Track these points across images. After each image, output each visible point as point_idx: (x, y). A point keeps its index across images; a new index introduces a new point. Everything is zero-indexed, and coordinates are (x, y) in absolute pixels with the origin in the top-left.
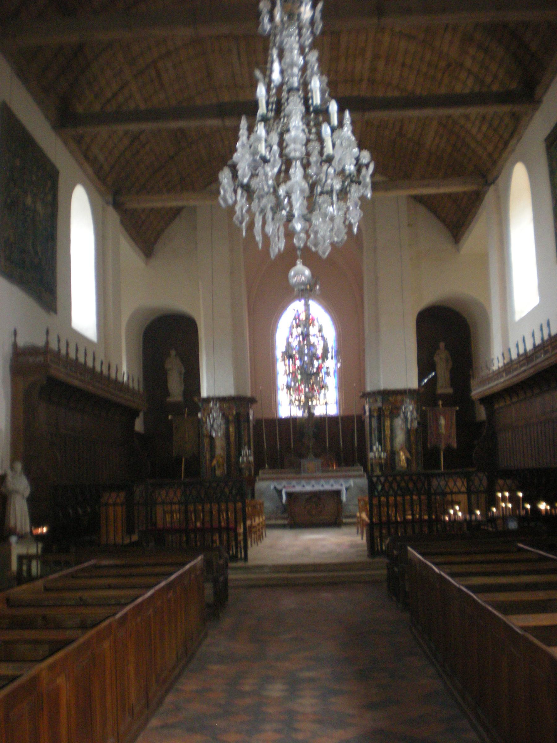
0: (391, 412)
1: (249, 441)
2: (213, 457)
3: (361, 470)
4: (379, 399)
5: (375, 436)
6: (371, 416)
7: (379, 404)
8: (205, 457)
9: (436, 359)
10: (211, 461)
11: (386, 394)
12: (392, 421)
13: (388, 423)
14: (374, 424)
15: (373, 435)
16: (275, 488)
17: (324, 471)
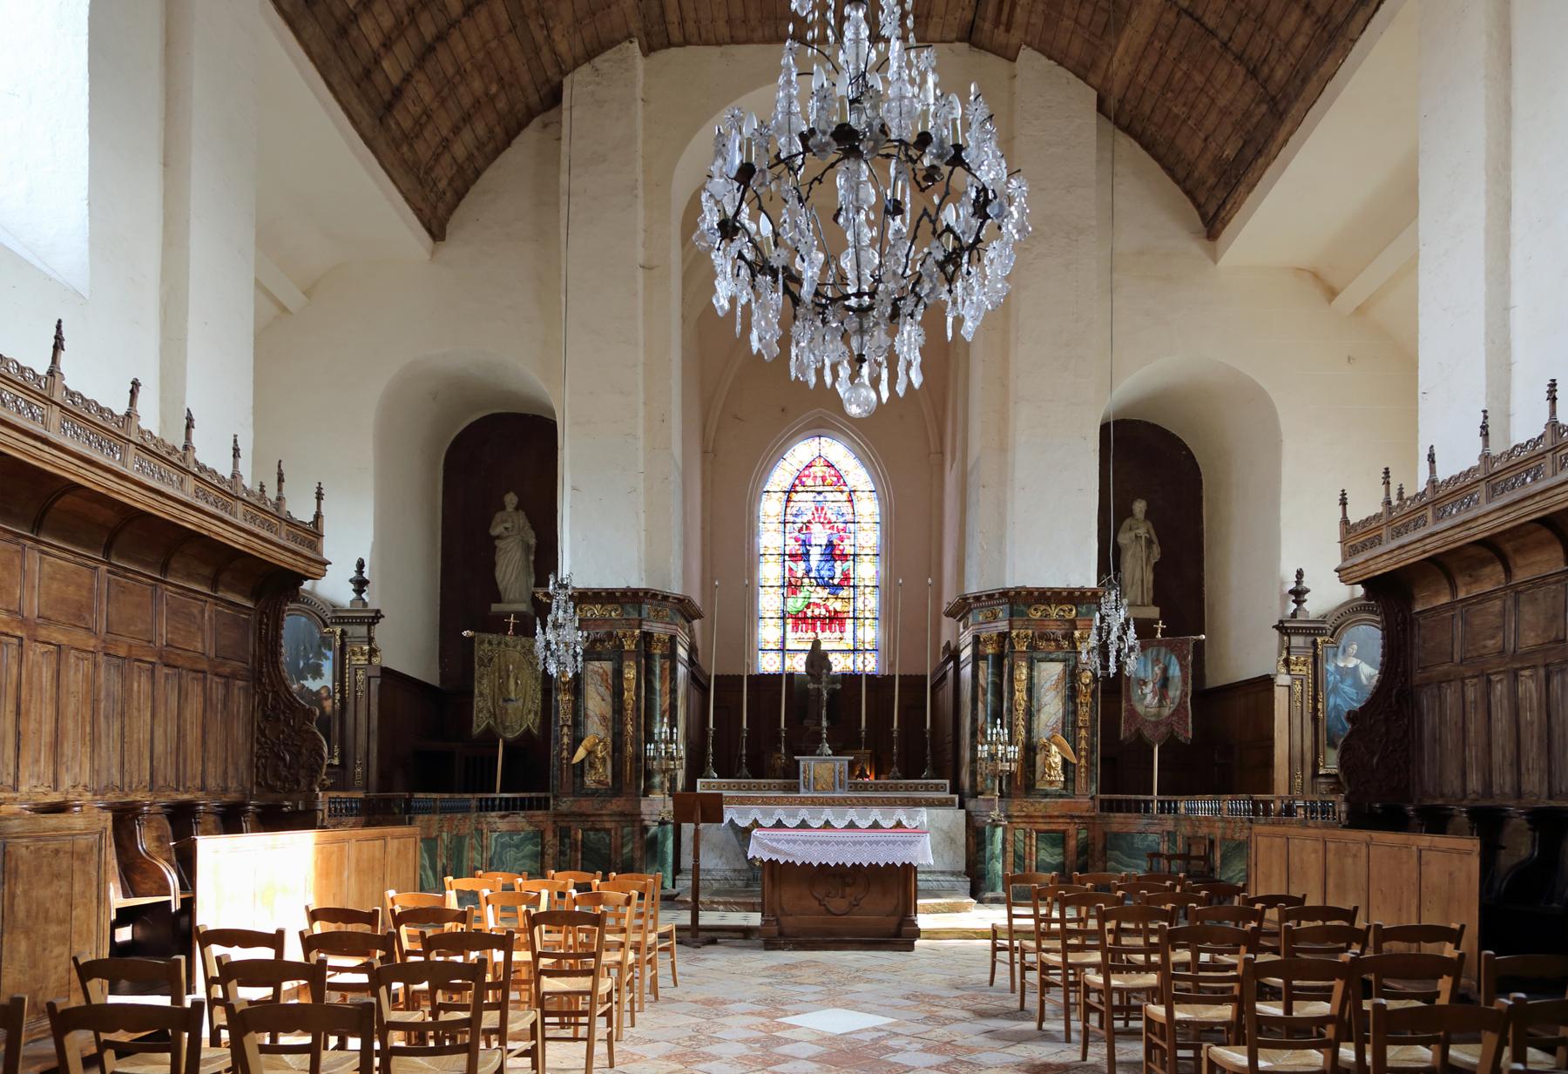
0: (1032, 647)
1: (673, 708)
2: (577, 742)
4: (1002, 611)
5: (986, 706)
6: (977, 657)
7: (1003, 626)
8: (559, 740)
9: (1123, 539)
10: (574, 752)
11: (1020, 600)
12: (1031, 669)
13: (1022, 673)
14: (986, 674)
15: (980, 705)
16: (731, 821)
17: (855, 787)
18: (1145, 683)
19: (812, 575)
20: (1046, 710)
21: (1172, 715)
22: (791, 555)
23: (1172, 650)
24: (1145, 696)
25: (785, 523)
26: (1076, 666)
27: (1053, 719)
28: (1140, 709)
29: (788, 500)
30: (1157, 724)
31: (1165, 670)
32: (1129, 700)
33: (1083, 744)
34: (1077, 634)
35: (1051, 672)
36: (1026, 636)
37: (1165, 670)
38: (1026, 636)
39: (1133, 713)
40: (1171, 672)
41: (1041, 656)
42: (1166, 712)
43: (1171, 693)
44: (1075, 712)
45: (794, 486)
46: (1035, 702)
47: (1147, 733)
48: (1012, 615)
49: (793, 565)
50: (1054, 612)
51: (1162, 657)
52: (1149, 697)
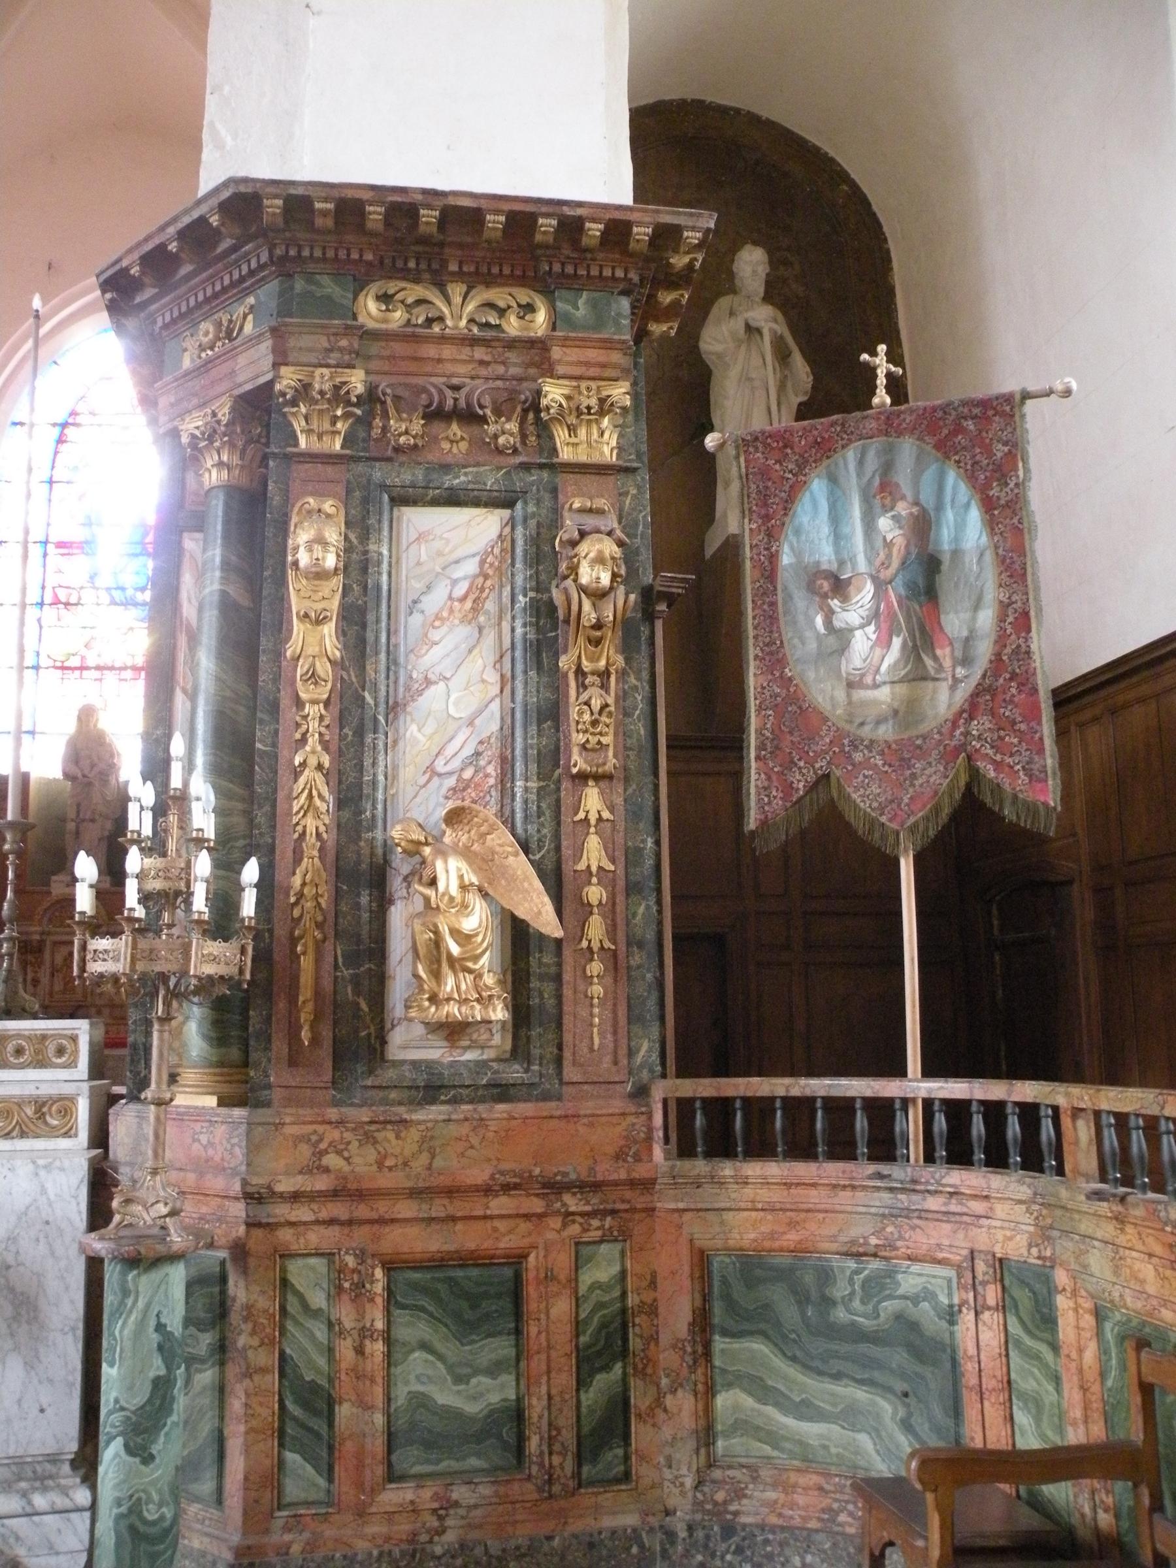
0: (366, 446)
3: (64, 1050)
12: (361, 526)
18: (839, 586)
19: (99, 582)
20: (432, 700)
21: (971, 710)
22: (60, 545)
23: (946, 449)
24: (842, 638)
25: (51, 482)
26: (555, 523)
27: (462, 745)
28: (825, 694)
29: (61, 440)
30: (901, 756)
31: (922, 526)
32: (775, 659)
33: (594, 854)
34: (554, 393)
35: (449, 548)
36: (339, 395)
37: (922, 526)
38: (339, 395)
39: (794, 709)
40: (945, 537)
41: (405, 476)
42: (944, 700)
43: (954, 622)
44: (550, 714)
45: (73, 413)
46: (377, 667)
47: (866, 796)
48: (284, 311)
49: (63, 562)
50: (459, 309)
51: (903, 477)
52: (862, 643)
